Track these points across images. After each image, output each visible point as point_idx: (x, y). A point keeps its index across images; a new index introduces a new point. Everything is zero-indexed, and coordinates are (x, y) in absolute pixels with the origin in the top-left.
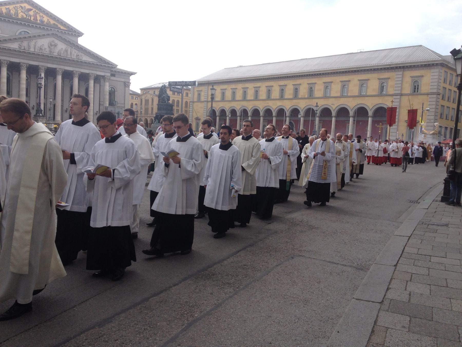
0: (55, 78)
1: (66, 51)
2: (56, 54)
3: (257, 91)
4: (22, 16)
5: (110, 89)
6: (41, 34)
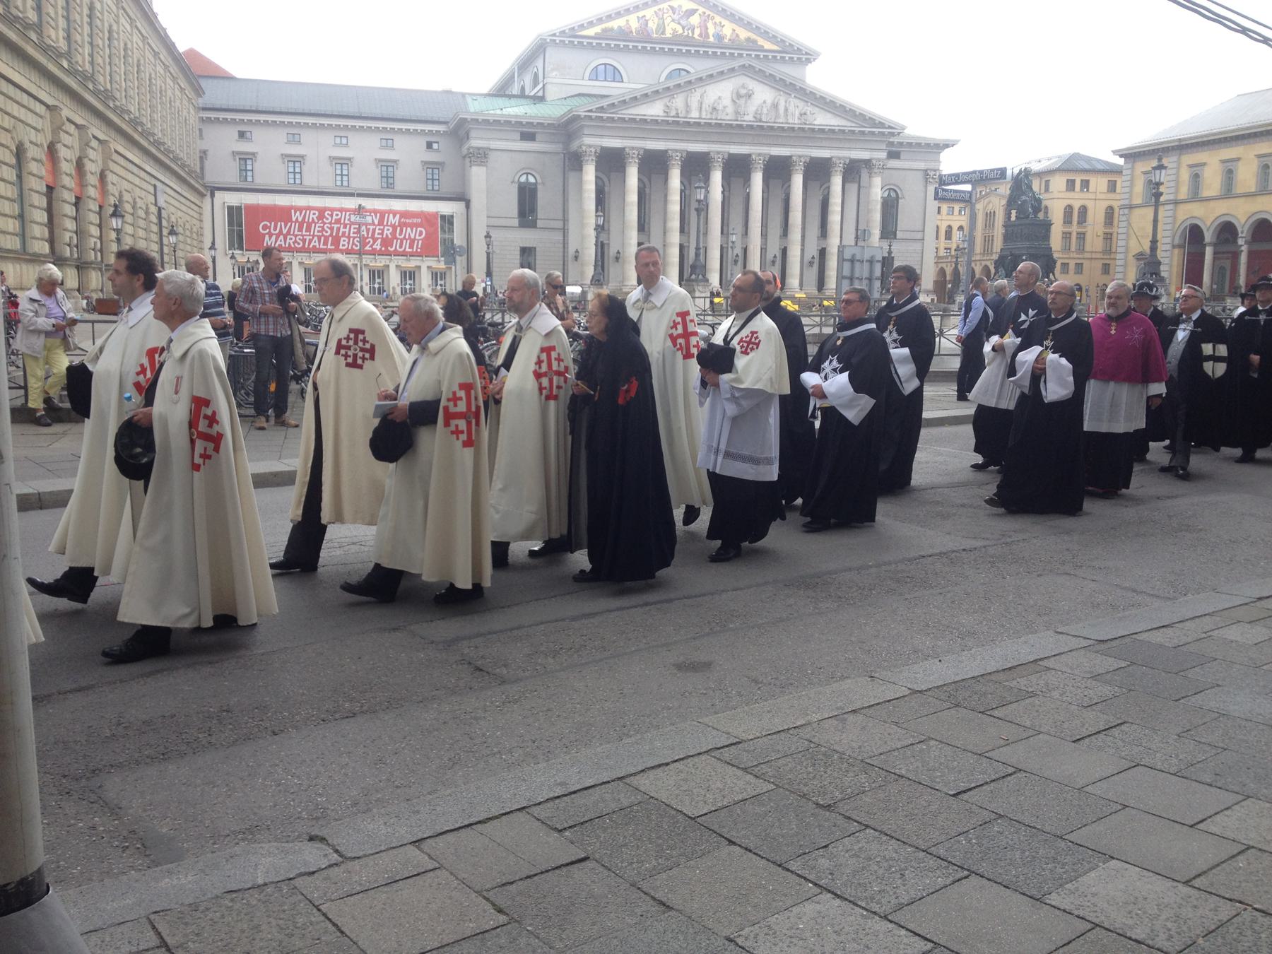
0: (747, 181)
1: (775, 106)
2: (749, 118)
3: (1230, 172)
4: (674, 31)
5: (886, 195)
6: (714, 72)
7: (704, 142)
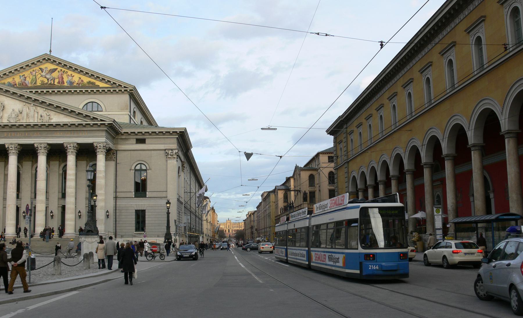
4: (42, 81)
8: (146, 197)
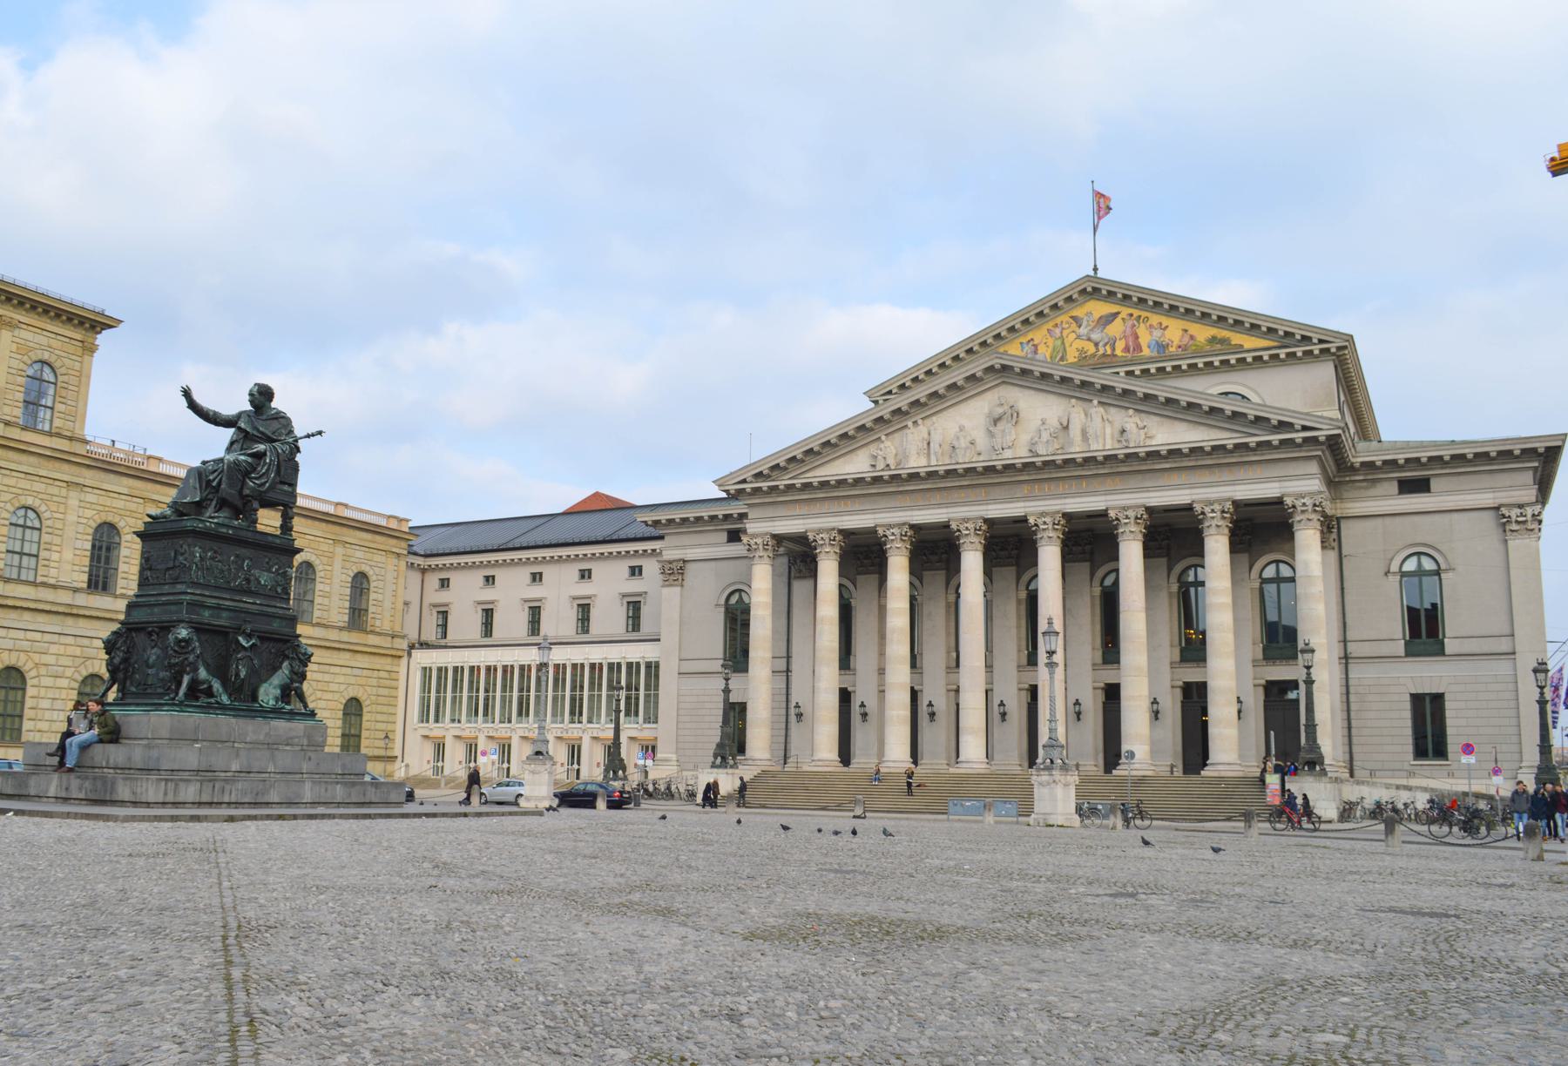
4: (1081, 351)
7: (939, 505)
8: (1441, 651)
